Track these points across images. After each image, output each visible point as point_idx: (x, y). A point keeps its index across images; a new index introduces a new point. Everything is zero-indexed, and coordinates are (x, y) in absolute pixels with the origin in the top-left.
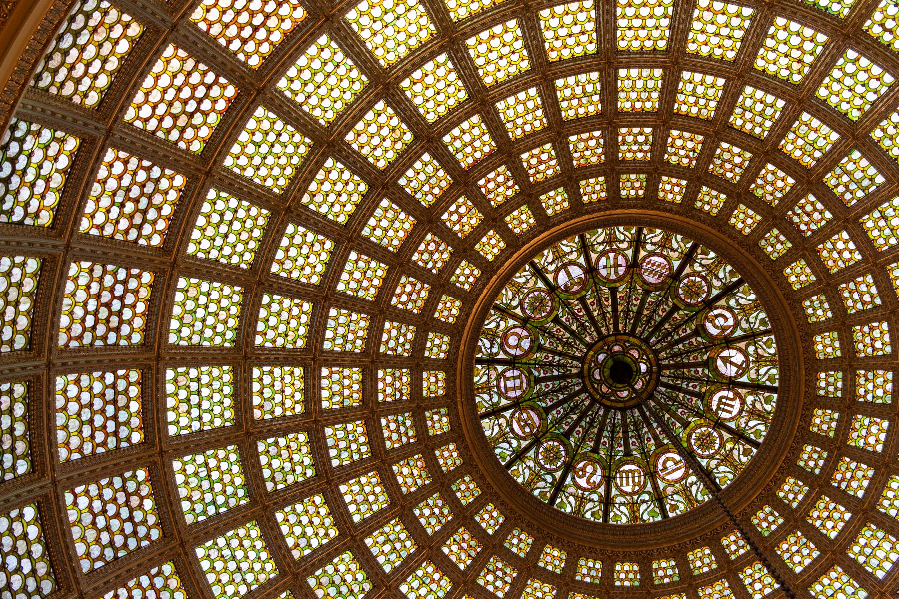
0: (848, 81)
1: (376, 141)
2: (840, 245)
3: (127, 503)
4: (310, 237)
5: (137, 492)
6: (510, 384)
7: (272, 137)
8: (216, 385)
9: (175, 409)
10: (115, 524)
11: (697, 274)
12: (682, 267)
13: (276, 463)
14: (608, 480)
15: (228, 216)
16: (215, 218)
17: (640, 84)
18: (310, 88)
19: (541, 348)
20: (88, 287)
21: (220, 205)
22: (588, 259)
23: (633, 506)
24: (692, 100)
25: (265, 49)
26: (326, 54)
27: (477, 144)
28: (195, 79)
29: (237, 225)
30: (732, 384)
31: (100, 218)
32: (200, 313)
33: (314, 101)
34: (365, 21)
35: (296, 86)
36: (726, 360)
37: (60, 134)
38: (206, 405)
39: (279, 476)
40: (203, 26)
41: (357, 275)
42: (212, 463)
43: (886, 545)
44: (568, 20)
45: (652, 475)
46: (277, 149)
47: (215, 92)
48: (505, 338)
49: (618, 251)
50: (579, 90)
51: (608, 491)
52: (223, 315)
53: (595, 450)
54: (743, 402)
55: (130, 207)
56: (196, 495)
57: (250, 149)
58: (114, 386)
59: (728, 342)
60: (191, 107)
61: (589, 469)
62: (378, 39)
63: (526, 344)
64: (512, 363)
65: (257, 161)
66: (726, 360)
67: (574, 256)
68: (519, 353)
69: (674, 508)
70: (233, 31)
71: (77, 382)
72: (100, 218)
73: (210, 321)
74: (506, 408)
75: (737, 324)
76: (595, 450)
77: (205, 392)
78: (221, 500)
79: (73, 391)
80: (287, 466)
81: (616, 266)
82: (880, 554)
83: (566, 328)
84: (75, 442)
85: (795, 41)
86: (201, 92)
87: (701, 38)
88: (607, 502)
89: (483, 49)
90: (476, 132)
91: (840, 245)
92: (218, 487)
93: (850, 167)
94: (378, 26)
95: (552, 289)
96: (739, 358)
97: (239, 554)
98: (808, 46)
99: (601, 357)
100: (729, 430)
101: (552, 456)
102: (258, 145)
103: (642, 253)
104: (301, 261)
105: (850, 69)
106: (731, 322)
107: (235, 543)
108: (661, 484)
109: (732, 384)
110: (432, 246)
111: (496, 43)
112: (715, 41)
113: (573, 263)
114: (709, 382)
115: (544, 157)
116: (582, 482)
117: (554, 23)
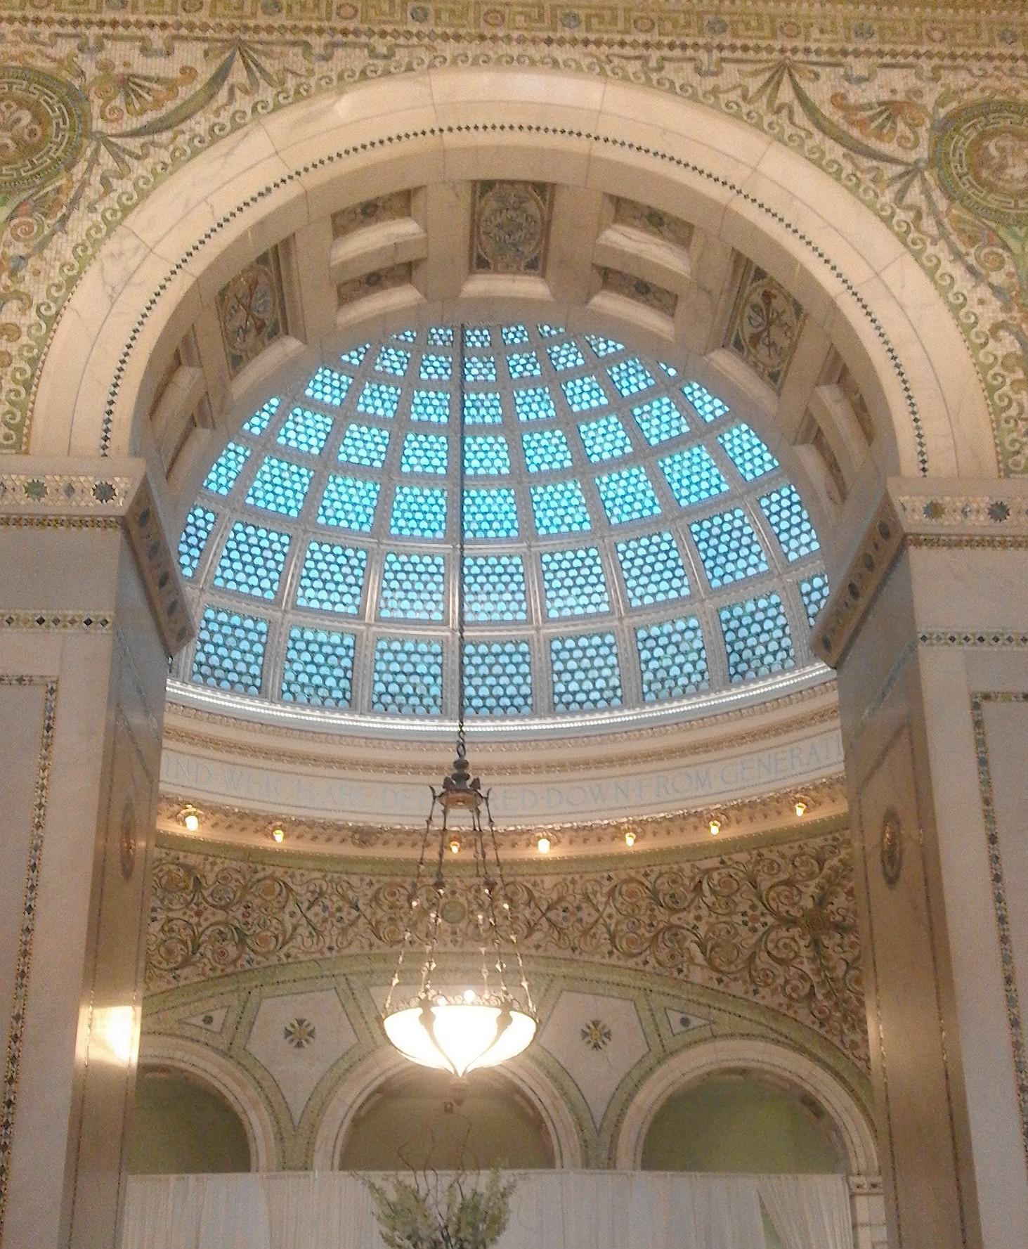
18: (705, 475)
26: (684, 492)
33: (705, 465)
34: (648, 503)
62: (641, 486)
86: (785, 514)
89: (559, 456)
111: (548, 458)
117: (498, 463)
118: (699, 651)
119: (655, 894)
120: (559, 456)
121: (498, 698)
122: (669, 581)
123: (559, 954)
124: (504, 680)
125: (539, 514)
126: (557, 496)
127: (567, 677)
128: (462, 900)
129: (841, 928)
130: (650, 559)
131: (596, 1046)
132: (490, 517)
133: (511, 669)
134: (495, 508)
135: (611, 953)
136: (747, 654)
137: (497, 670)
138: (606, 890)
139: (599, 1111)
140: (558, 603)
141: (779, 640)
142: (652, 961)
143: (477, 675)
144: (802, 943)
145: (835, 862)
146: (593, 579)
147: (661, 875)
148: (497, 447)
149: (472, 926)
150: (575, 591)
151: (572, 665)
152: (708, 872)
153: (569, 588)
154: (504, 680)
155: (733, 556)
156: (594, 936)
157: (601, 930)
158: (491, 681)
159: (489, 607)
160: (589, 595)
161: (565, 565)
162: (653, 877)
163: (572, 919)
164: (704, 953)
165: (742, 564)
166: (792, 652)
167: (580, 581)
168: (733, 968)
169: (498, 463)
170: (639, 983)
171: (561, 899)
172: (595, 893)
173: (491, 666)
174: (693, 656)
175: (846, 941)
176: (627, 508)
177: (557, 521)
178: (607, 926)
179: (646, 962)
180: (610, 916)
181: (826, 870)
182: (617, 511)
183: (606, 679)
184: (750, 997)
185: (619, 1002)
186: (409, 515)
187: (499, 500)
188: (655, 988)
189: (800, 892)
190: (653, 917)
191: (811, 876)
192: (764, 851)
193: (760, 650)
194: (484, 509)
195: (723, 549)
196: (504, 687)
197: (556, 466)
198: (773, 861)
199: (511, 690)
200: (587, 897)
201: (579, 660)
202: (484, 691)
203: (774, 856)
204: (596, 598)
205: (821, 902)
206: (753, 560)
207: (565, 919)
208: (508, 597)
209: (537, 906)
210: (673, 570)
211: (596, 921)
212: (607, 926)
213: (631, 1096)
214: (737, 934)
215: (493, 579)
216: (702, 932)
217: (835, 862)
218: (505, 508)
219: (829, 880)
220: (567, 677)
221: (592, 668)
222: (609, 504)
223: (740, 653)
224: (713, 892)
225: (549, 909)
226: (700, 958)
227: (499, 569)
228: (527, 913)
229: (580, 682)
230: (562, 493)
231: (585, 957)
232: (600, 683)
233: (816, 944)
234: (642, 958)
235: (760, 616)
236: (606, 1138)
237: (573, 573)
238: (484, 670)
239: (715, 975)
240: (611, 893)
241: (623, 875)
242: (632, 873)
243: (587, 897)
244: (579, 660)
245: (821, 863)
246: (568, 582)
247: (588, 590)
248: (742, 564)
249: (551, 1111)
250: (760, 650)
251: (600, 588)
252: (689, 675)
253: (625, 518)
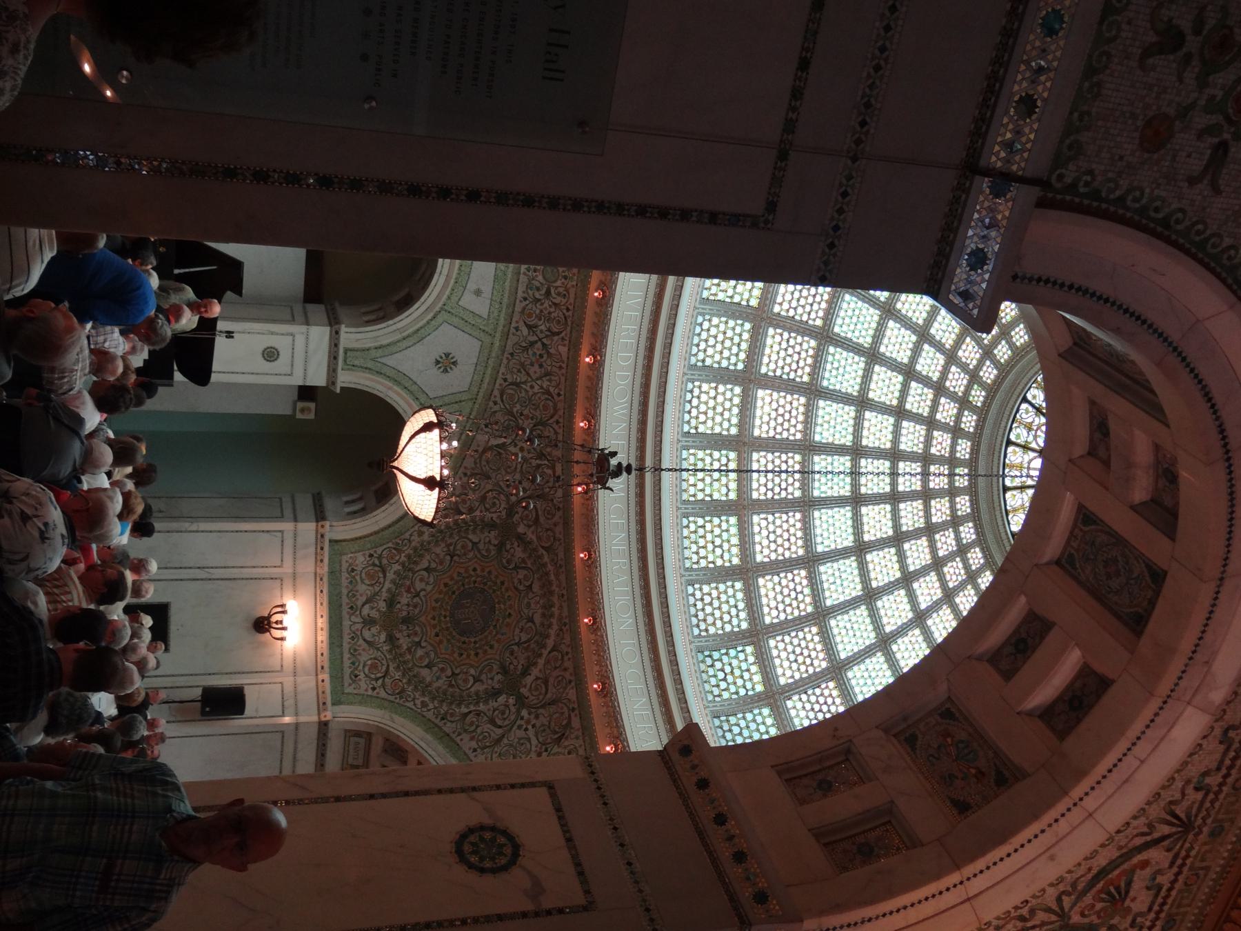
1: (878, 526)
7: (837, 574)
16: (844, 632)
17: (929, 361)
18: (832, 537)
20: (804, 708)
25: (800, 543)
28: (784, 582)
31: (789, 673)
33: (839, 540)
37: (740, 649)
40: (766, 560)
47: (797, 579)
50: (918, 398)
60: (793, 594)
62: (836, 488)
65: (840, 590)
67: (1026, 458)
70: (780, 550)
72: (789, 673)
87: (917, 314)
89: (872, 437)
110: (943, 539)
113: (1031, 461)
115: (940, 439)
117: (879, 392)
118: (711, 496)
119: (543, 424)
120: (872, 437)
121: (706, 341)
122: (766, 485)
123: (510, 343)
124: (719, 347)
125: (835, 405)
126: (845, 425)
127: (712, 393)
128: (559, 283)
129: (500, 546)
131: (437, 362)
132: (841, 370)
133: (726, 353)
134: (847, 376)
135: (505, 380)
136: (701, 532)
137: (728, 343)
138: (551, 389)
139: (390, 361)
140: (768, 399)
141: (706, 558)
142: (496, 408)
143: (727, 328)
144: (495, 516)
145: (546, 559)
146: (779, 429)
147: (556, 433)
149: (538, 284)
150: (773, 415)
151: (720, 399)
152: (553, 468)
153: (776, 410)
154: (719, 347)
156: (519, 371)
157: (521, 377)
158: (721, 337)
159: (776, 348)
160: (768, 423)
161: (794, 413)
162: (555, 426)
163: (534, 359)
164: (497, 446)
165: (765, 543)
166: (695, 566)
167: (780, 420)
168: (484, 463)
169: (879, 392)
170: (481, 394)
171: (548, 352)
172: (550, 381)
173: (732, 339)
174: (708, 491)
175: (492, 547)
178: (525, 383)
179: (495, 403)
180: (532, 387)
181: (542, 551)
183: (705, 422)
184: (462, 469)
185: (469, 379)
186: (857, 312)
188: (477, 406)
189: (529, 526)
190: (527, 417)
191: (539, 538)
192: (560, 514)
193: (702, 542)
194: (848, 368)
195: (779, 531)
196: (714, 346)
198: (554, 515)
199: (710, 351)
200: (547, 374)
201: (722, 404)
202: (713, 331)
203: (556, 519)
204: (765, 427)
205: (520, 538)
206: (766, 552)
207: (535, 354)
208: (781, 363)
209: (547, 336)
210: (772, 490)
211: (528, 374)
212: (525, 383)
213: (398, 383)
214: (507, 473)
215: (796, 357)
216: (512, 449)
217: (546, 559)
218: (845, 384)
219: (535, 550)
220: (712, 393)
221: (715, 414)
223: (703, 527)
224: (539, 466)
225: (544, 344)
226: (494, 442)
227: (802, 364)
228: (543, 327)
229: (706, 403)
231: (505, 361)
232: (702, 418)
233: (492, 526)
234: (498, 399)
235: (726, 546)
236: (370, 364)
237: (787, 416)
238: (730, 334)
239: (481, 449)
240: (548, 392)
241: (560, 405)
242: (561, 413)
243: (547, 374)
244: (722, 404)
245: (547, 549)
246: (781, 411)
247: (773, 424)
248: (765, 543)
249: (394, 327)
250: (702, 542)
252: (695, 485)
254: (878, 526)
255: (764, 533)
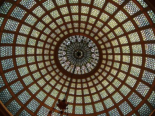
0: (94, 12)
1: (35, 35)
2: (100, 33)
3: (18, 85)
4: (31, 48)
5: (19, 84)
6: (64, 59)
7: (21, 38)
8: (25, 69)
9: (21, 73)
10: (18, 88)
11: (85, 39)
12: (83, 39)
13: (36, 76)
14: (81, 68)
15: (19, 49)
19: (67, 53)
21: (18, 48)
22: (70, 41)
23: (84, 71)
24: (75, 19)
27: (49, 31)
29: (21, 50)
30: (93, 53)
32: (20, 61)
34: (27, 21)
35: (22, 31)
36: (92, 50)
38: (25, 72)
39: (36, 78)
41: (39, 51)
42: (28, 78)
43: (115, 71)
44: (54, 13)
45: (86, 67)
46: (23, 39)
48: (62, 53)
49: (74, 39)
50: (59, 21)
51: (81, 70)
52: (23, 61)
53: (78, 65)
54: (96, 55)
55: (6, 52)
56: (27, 82)
57: (19, 40)
58: (12, 73)
59: (92, 48)
61: (78, 67)
63: (65, 53)
64: (64, 56)
66: (92, 50)
68: (65, 55)
69: (90, 70)
71: (8, 73)
72: (3, 55)
73: (22, 62)
74: (65, 62)
75: (92, 45)
76: (78, 65)
77: (24, 70)
78: (30, 82)
79: (7, 75)
80: (37, 76)
81: (74, 41)
82: (115, 72)
83: (70, 50)
84: (10, 80)
85: (85, 8)
88: (81, 71)
89: (44, 19)
90: (48, 30)
91: (100, 33)
92: (29, 81)
93: (98, 23)
94: (29, 21)
95: (67, 45)
96: (94, 49)
97: (34, 88)
98: (87, 9)
99: (76, 53)
100: (95, 59)
101: (72, 67)
102: (20, 40)
103: (77, 38)
104: (31, 52)
105: (94, 10)
106: (91, 45)
107: (33, 86)
108: (88, 68)
109: (93, 53)
110: (47, 45)
111: (46, 18)
112: (75, 11)
113: (68, 42)
114: (91, 53)
116: (77, 69)
126: (41, 13)
130: (20, 14)
146: (26, 5)
148: (54, 16)
155: (10, 25)
165: (8, 26)
169: (53, 14)
176: (30, 18)
177: (38, 10)
182: (31, 17)
187: (49, 8)
197: (44, 18)
222: (33, 17)
230: (40, 14)
247: (25, 3)
251: (24, 5)
253: (29, 17)
254: (35, 35)
255: (9, 24)
